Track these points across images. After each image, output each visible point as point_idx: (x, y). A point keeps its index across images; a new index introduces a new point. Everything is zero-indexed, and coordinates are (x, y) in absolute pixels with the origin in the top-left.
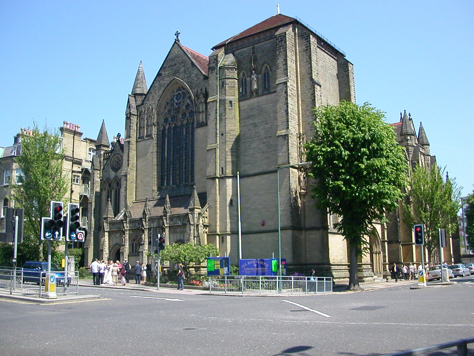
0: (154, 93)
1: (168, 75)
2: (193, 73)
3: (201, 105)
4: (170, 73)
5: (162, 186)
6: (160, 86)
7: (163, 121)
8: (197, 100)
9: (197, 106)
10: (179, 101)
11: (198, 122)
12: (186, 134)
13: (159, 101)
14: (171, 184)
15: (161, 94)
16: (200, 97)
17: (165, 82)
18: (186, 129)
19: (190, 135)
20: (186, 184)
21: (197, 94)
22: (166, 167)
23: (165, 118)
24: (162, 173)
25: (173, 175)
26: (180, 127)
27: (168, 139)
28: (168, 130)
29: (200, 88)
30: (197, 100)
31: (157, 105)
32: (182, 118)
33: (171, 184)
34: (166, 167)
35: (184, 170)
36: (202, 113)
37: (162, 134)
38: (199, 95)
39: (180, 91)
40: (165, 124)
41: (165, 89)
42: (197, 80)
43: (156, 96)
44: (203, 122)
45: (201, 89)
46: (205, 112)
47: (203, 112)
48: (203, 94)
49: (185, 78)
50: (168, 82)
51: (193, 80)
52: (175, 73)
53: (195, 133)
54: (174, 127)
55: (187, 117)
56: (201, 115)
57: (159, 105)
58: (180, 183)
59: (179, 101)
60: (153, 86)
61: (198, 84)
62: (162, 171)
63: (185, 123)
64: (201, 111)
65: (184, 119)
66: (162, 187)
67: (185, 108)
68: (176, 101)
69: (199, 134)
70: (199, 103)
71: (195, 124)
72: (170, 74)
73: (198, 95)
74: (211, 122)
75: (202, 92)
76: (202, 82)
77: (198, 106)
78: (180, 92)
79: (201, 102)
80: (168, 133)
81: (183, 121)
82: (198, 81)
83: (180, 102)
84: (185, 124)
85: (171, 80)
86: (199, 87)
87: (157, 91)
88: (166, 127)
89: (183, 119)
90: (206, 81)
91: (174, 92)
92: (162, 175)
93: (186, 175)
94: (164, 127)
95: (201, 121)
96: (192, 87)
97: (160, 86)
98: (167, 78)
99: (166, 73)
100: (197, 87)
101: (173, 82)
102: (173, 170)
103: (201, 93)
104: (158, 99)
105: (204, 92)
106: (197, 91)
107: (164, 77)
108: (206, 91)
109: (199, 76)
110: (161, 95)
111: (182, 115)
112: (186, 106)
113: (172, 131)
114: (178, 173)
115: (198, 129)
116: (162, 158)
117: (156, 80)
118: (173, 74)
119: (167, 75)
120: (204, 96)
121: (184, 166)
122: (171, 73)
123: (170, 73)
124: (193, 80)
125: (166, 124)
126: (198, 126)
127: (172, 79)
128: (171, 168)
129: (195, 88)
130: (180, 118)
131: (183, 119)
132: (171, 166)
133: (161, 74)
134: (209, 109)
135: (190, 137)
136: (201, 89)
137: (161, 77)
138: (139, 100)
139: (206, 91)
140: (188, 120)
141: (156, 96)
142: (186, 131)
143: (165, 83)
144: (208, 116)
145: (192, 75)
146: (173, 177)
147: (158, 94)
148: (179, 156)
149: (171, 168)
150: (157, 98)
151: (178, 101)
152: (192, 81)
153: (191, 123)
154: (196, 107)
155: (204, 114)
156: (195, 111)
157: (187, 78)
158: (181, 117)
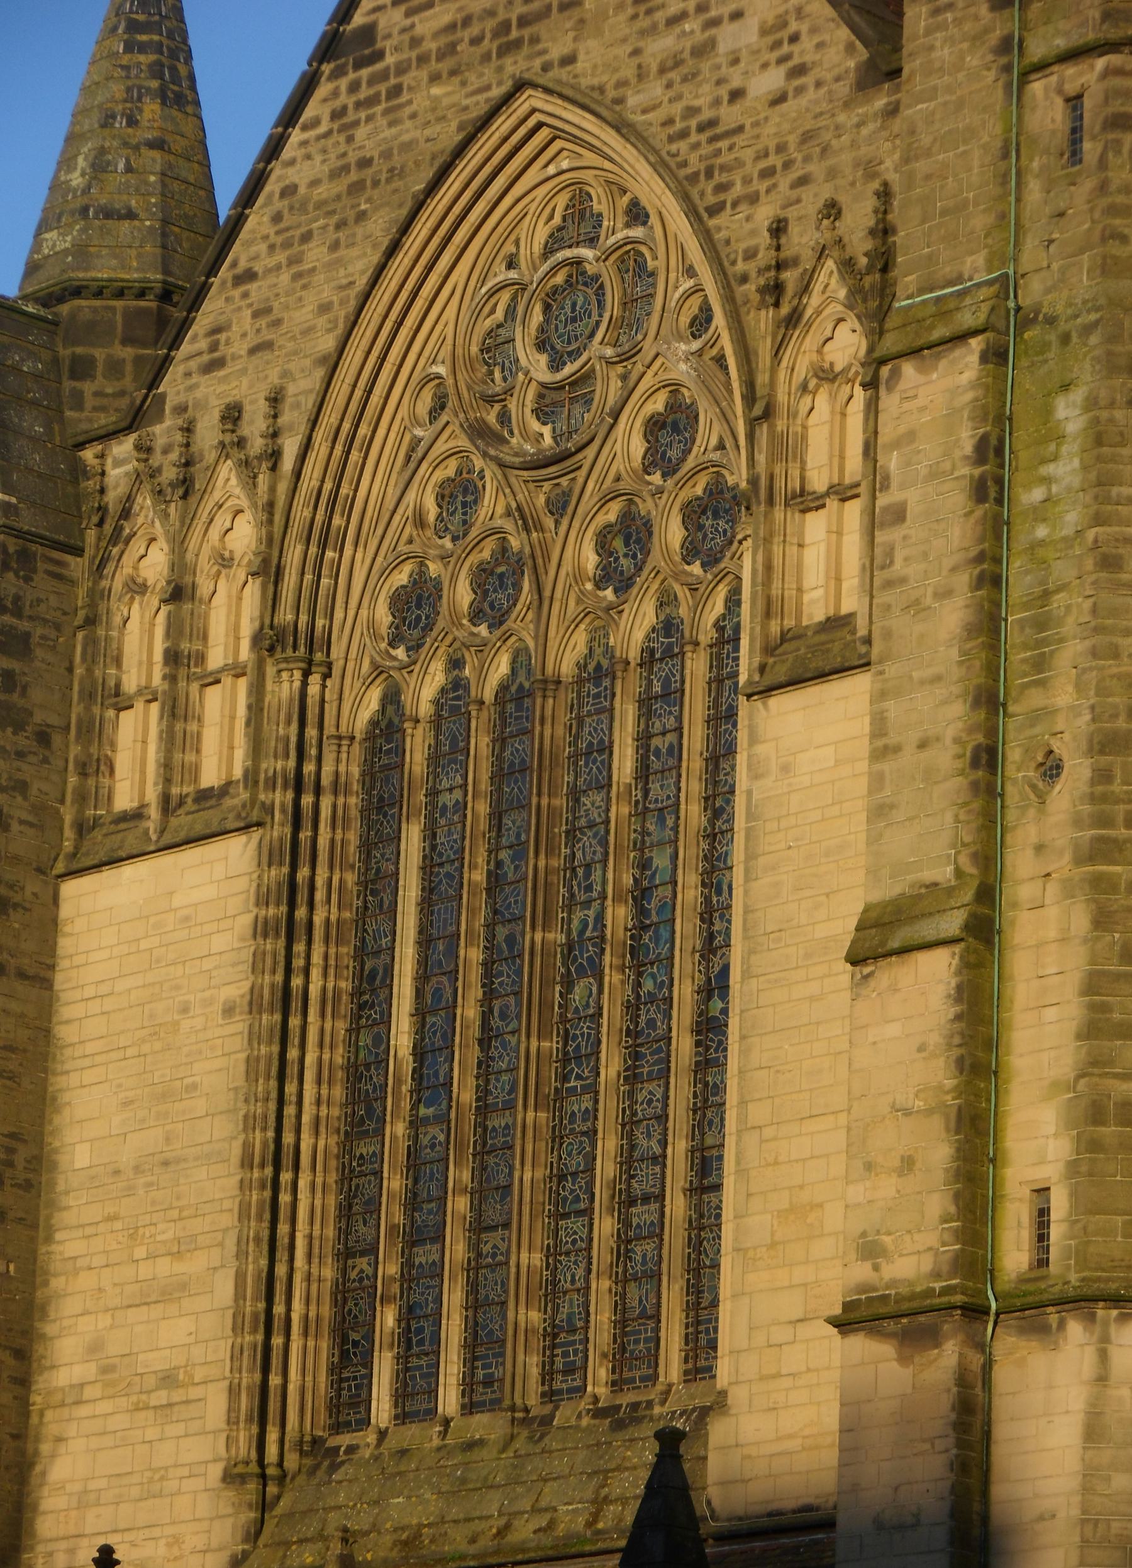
0: (285, 278)
1: (451, 49)
2: (737, 15)
3: (822, 401)
4: (467, 21)
5: (338, 1428)
6: (356, 188)
7: (383, 616)
8: (777, 354)
9: (768, 414)
10: (568, 369)
11: (775, 628)
12: (643, 772)
13: (333, 364)
14: (449, 1399)
15: (362, 282)
16: (814, 300)
17: (409, 131)
18: (646, 705)
19: (693, 786)
20: (625, 1399)
21: (779, 266)
22: (394, 1183)
23: (402, 577)
24: (345, 1255)
25: (473, 1288)
26: (580, 681)
27: (430, 834)
28: (437, 722)
29: (812, 200)
30: (777, 354)
31: (314, 423)
32: (599, 585)
33: (449, 1399)
34: (394, 1183)
35: (605, 1226)
36: (832, 504)
37: (369, 775)
38: (805, 289)
39: (592, 242)
40: (400, 653)
41: (405, 228)
42: (780, 99)
43: (304, 315)
44: (838, 623)
45: (832, 210)
46: (863, 489)
47: (843, 493)
48: (847, 265)
49: (641, 74)
50: (449, 135)
51: (736, 95)
52: (523, 22)
53: (741, 759)
54: (503, 688)
55: (656, 558)
56: (816, 525)
57: (329, 419)
58: (550, 1396)
59: (568, 369)
60: (272, 186)
61: (792, 140)
62: (344, 1233)
63: (639, 636)
64: (818, 482)
65: (624, 586)
66: (344, 1440)
67: (638, 447)
68: (538, 366)
69: (785, 769)
70: (804, 388)
71: (744, 642)
72: (467, 34)
73: (790, 277)
74: (915, 607)
75: (840, 241)
76: (842, 118)
77: (780, 425)
78: (587, 253)
79: (826, 375)
80: (435, 759)
81: (614, 610)
82: (791, 106)
83: (585, 378)
84: (634, 655)
85: (479, 105)
86: (803, 181)
87: (316, 253)
88: (407, 698)
89: (609, 594)
90: (880, 102)
91: (511, 264)
92: (342, 1293)
93: (623, 1280)
94: (392, 698)
95: (816, 611)
96: (722, 188)
97: (356, 188)
98: (435, 78)
99: (429, 23)
100: (784, 182)
101: (502, 125)
102: (478, 1227)
103: (821, 254)
104: (327, 343)
105: (860, 245)
106: (778, 229)
107: (402, 69)
108: (883, 231)
109: (807, 43)
110: (366, 296)
111: (602, 544)
112: (654, 426)
113: (481, 743)
114: (531, 1259)
115: (779, 702)
116: (356, 1073)
117: (308, 113)
118: (505, 26)
119: (431, 46)
120: (857, 296)
121: (606, 1168)
122: (490, 24)
123: (467, 21)
124: (736, 95)
125: (414, 648)
126: (781, 673)
127: (496, 92)
128: (459, 1205)
129: (753, 199)
130: (578, 576)
131: (609, 594)
132: (460, 1174)
133: (368, 33)
134: (896, 444)
135: (693, 814)
136: (832, 210)
137: (365, 73)
138: (115, 368)
139: (883, 231)
140: (666, 600)
141: (304, 315)
142: (643, 739)
143: (407, 147)
144: (881, 537)
145: (729, 37)
146: (475, 1304)
147: (324, 290)
148: (551, 1045)
149: (459, 1205)
150: (308, 331)
151: (556, 365)
152: (730, 115)
153: (707, 634)
154: (763, 432)
155: (854, 511)
156: (754, 481)
157: (662, 71)
158: (590, 560)
